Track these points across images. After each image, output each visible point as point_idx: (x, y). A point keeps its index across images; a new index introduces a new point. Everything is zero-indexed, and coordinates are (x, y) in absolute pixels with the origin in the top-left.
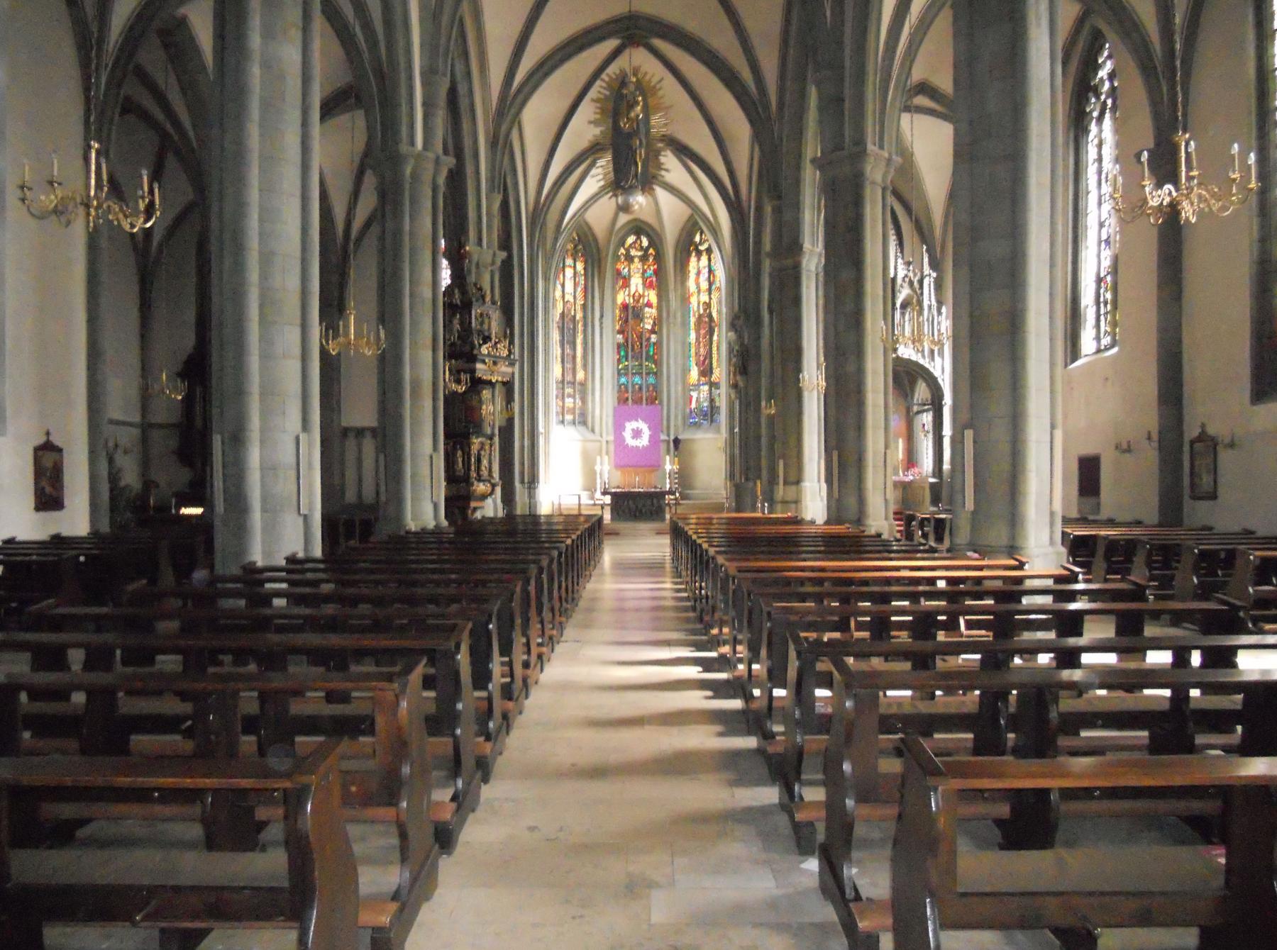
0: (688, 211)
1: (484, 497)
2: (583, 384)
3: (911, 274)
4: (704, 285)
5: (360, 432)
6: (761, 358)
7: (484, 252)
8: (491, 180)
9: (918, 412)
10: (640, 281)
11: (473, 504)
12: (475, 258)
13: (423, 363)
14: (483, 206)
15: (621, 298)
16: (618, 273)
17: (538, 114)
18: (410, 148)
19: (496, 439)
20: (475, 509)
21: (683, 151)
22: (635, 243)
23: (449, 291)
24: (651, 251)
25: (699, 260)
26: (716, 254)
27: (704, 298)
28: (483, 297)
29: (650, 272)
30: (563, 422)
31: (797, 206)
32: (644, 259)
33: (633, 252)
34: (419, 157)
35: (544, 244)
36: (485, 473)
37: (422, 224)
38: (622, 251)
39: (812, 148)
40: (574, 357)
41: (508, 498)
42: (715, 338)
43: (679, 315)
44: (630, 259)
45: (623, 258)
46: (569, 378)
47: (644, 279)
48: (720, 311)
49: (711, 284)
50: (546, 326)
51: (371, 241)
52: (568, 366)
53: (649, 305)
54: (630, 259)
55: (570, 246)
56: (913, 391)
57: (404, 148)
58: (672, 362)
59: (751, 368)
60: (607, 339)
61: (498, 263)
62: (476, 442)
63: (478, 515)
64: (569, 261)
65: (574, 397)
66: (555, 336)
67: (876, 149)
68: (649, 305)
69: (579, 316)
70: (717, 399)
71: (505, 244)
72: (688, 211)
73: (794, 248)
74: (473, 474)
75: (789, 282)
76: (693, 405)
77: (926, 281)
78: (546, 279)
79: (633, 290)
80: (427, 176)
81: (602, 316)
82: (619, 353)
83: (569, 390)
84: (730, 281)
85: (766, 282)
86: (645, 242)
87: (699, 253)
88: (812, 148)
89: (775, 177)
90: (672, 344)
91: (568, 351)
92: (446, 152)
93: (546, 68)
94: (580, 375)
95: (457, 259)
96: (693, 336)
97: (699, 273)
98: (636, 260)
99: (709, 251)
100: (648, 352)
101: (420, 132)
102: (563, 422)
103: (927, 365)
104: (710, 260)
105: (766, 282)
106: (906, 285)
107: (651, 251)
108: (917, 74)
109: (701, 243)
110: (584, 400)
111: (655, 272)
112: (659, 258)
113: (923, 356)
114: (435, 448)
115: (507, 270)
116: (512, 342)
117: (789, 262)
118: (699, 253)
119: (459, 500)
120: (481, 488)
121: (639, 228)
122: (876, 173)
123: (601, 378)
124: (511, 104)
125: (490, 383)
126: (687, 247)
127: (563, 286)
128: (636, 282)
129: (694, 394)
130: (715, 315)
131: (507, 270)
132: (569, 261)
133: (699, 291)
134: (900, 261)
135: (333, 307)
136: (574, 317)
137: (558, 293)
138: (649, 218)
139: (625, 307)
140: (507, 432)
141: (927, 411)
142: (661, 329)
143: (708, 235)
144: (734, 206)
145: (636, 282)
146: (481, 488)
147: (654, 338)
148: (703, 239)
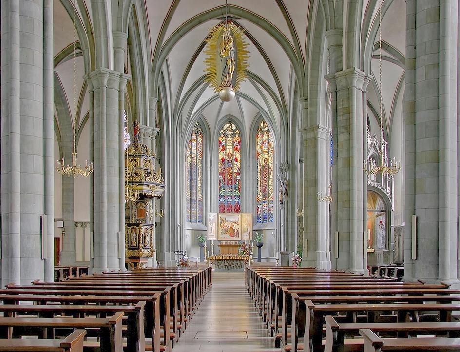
0: (257, 110)
1: (148, 257)
2: (202, 201)
3: (375, 142)
4: (265, 149)
5: (84, 224)
6: (296, 188)
7: (148, 129)
8: (151, 91)
9: (377, 216)
10: (231, 147)
11: (141, 261)
12: (143, 131)
13: (113, 185)
14: (147, 105)
15: (221, 156)
16: (220, 142)
17: (176, 57)
18: (107, 69)
19: (154, 226)
20: (142, 264)
21: (254, 78)
22: (229, 127)
23: (129, 150)
24: (237, 132)
25: (263, 136)
26: (272, 133)
27: (265, 156)
28: (147, 151)
29: (236, 143)
30: (190, 221)
31: (315, 105)
32: (233, 136)
33: (228, 132)
34: (110, 74)
35: (181, 127)
36: (148, 246)
37: (113, 109)
38: (222, 131)
39: (325, 70)
40: (197, 186)
41: (160, 259)
42: (271, 177)
43: (251, 165)
44: (226, 136)
45: (222, 136)
46: (194, 198)
47: (234, 146)
48: (273, 162)
49: (268, 149)
50: (181, 171)
51: (88, 125)
52: (193, 191)
53: (236, 160)
54: (226, 136)
55: (194, 129)
56: (375, 204)
57: (103, 69)
58: (248, 189)
59: (290, 192)
60: (214, 178)
61: (156, 133)
62: (143, 228)
63: (144, 266)
64: (194, 137)
65: (197, 207)
66: (186, 175)
67: (359, 70)
68: (236, 160)
69: (199, 165)
70: (272, 209)
71: (160, 124)
72: (257, 110)
73: (314, 128)
74: (142, 245)
75: (311, 145)
76: (259, 213)
77: (382, 146)
78: (181, 145)
79: (228, 151)
80: (116, 86)
81: (211, 165)
82: (220, 185)
83: (193, 204)
84: (279, 147)
85: (298, 146)
86: (234, 127)
87: (263, 133)
88: (325, 70)
89: (304, 90)
90: (248, 181)
91: (193, 184)
92: (126, 72)
93: (181, 33)
94: (199, 197)
95: (135, 131)
96: (259, 176)
97: (263, 142)
98: (229, 136)
99: (268, 132)
100: (235, 185)
101: (112, 61)
102: (190, 221)
103: (383, 190)
104: (268, 136)
105: (298, 146)
106: (372, 148)
107: (237, 132)
108: (379, 39)
109: (264, 127)
110: (202, 210)
111: (239, 142)
112: (241, 135)
113: (381, 187)
114: (120, 230)
115: (160, 136)
116: (162, 176)
117: (310, 135)
118: (263, 133)
119: (134, 260)
120: (146, 252)
121: (230, 120)
122: (358, 84)
123: (211, 197)
124: (161, 52)
125: (151, 197)
126: (256, 129)
127: (191, 150)
128: (229, 148)
129: (260, 207)
130: (270, 165)
131: (160, 136)
132: (194, 137)
133: (263, 152)
134: (369, 135)
135: (65, 156)
136: (197, 166)
137: (188, 154)
138: (236, 114)
139: (223, 160)
140: (160, 224)
141: (381, 215)
142: (242, 172)
143: (268, 123)
144: (282, 107)
145: (229, 148)
146: (146, 252)
147: (238, 177)
148: (266, 126)
